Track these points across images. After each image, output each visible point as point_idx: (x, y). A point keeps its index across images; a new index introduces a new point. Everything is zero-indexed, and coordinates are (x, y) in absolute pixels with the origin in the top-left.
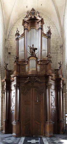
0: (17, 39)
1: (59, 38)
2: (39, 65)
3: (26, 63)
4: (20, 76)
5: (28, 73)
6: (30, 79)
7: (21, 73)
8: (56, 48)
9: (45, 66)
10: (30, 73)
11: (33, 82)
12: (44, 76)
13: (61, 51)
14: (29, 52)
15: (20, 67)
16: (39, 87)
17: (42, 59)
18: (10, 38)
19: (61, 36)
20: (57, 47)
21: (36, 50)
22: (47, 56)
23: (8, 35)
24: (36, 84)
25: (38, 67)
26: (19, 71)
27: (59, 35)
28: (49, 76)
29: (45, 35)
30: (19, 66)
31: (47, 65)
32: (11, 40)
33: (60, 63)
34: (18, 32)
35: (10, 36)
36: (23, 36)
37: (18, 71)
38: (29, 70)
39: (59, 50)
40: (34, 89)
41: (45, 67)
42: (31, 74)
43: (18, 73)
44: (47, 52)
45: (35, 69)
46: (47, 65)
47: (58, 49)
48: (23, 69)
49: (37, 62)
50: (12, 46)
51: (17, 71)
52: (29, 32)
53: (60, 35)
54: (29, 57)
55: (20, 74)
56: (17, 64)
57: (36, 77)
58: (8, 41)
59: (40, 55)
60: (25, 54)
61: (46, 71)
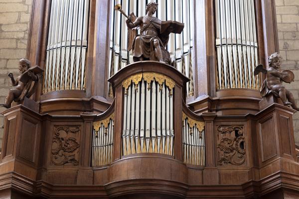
2: (201, 125)
5: (110, 175)
7: (51, 169)
9: (246, 131)
10: (126, 170)
14: (119, 54)
15: (51, 135)
17: (219, 96)
21: (171, 35)
22: (260, 69)
25: (194, 139)
38: (118, 152)
41: (247, 137)
42: (132, 177)
43: (33, 173)
45: (167, 148)
48: (71, 145)
49: (185, 111)
54: (124, 73)
55: (44, 178)
56: (28, 114)
60: (89, 61)
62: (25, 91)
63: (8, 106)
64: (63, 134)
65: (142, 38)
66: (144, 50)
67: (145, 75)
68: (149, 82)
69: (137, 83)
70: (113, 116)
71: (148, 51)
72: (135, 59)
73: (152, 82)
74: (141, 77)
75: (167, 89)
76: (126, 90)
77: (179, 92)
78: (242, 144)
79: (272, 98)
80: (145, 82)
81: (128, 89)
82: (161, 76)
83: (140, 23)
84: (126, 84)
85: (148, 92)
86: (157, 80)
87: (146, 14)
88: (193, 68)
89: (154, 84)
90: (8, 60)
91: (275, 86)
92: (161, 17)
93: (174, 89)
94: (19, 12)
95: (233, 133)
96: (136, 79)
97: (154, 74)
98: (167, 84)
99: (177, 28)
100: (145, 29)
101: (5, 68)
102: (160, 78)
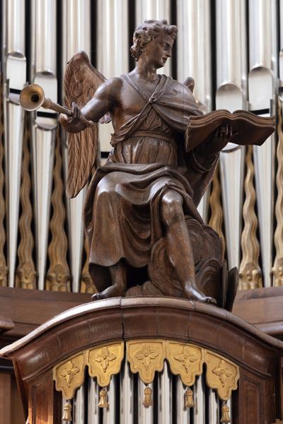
65: (118, 189)
66: (129, 235)
67: (135, 348)
68: (147, 377)
69: (106, 380)
71: (145, 235)
73: (158, 375)
74: (120, 357)
75: (212, 395)
76: (66, 405)
80: (135, 378)
81: (72, 401)
82: (192, 351)
83: (111, 105)
84: (67, 375)
86: (176, 368)
87: (131, 67)
89: (165, 381)
93: (235, 395)
96: (103, 361)
97: (166, 343)
98: (213, 382)
100: (129, 137)
102: (186, 358)
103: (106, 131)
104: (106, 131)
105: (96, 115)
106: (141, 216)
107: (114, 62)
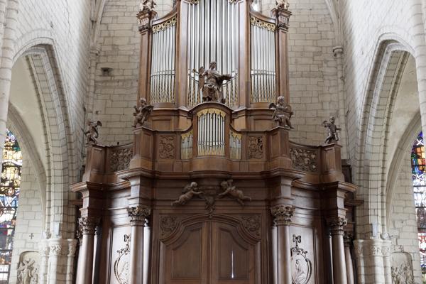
0: (148, 30)
1: (329, 21)
2: (239, 136)
3: (184, 123)
4: (157, 175)
6: (197, 186)
8: (316, 58)
9: (264, 139)
10: (200, 166)
11: (211, 200)
12: (258, 176)
13: (336, 68)
15: (159, 142)
16: (239, 218)
18: (115, 15)
19: (333, 15)
20: (319, 53)
23: (105, 5)
24: (222, 208)
25: (236, 143)
26: (151, 156)
27: (327, 8)
28: (279, 177)
29: (261, 19)
30: (151, 137)
31: (271, 137)
32: (115, 21)
33: (332, 127)
34: (148, 4)
35: (114, 9)
36: (174, 22)
37: (152, 157)
39: (329, 64)
40: (215, 226)
41: (264, 143)
42: (203, 169)
43: (150, 163)
44: (272, 79)
45: (221, 151)
46: (271, 137)
47: (326, 61)
48: (170, 147)
49: (231, 116)
50: (117, 46)
51: (146, 157)
52: (196, 5)
53: (329, 8)
57: (226, 179)
58: (104, 27)
59: (243, 90)
60: (177, 84)
61: (269, 159)
62: (144, 118)
63: (135, 127)
64: (165, 141)
69: (205, 114)
70: (192, 131)
72: (204, 99)
77: (228, 120)
78: (261, 147)
79: (278, 123)
83: (207, 74)
84: (199, 114)
85: (211, 120)
88: (237, 88)
90: (124, 70)
91: (280, 116)
92: (219, 72)
94: (130, 37)
95: (257, 141)
96: (205, 111)
99: (228, 78)
101: (123, 75)
102: (218, 111)
103: (206, 78)
104: (206, 78)
105: (204, 75)
106: (211, 90)
107: (207, 68)
